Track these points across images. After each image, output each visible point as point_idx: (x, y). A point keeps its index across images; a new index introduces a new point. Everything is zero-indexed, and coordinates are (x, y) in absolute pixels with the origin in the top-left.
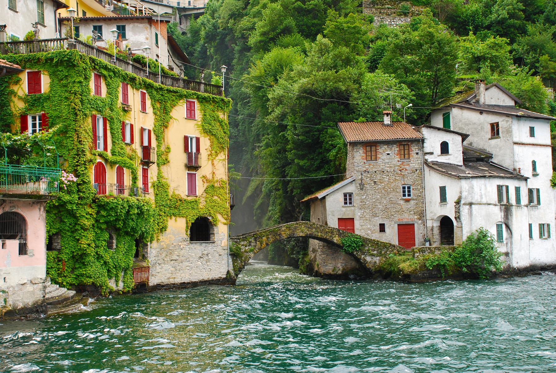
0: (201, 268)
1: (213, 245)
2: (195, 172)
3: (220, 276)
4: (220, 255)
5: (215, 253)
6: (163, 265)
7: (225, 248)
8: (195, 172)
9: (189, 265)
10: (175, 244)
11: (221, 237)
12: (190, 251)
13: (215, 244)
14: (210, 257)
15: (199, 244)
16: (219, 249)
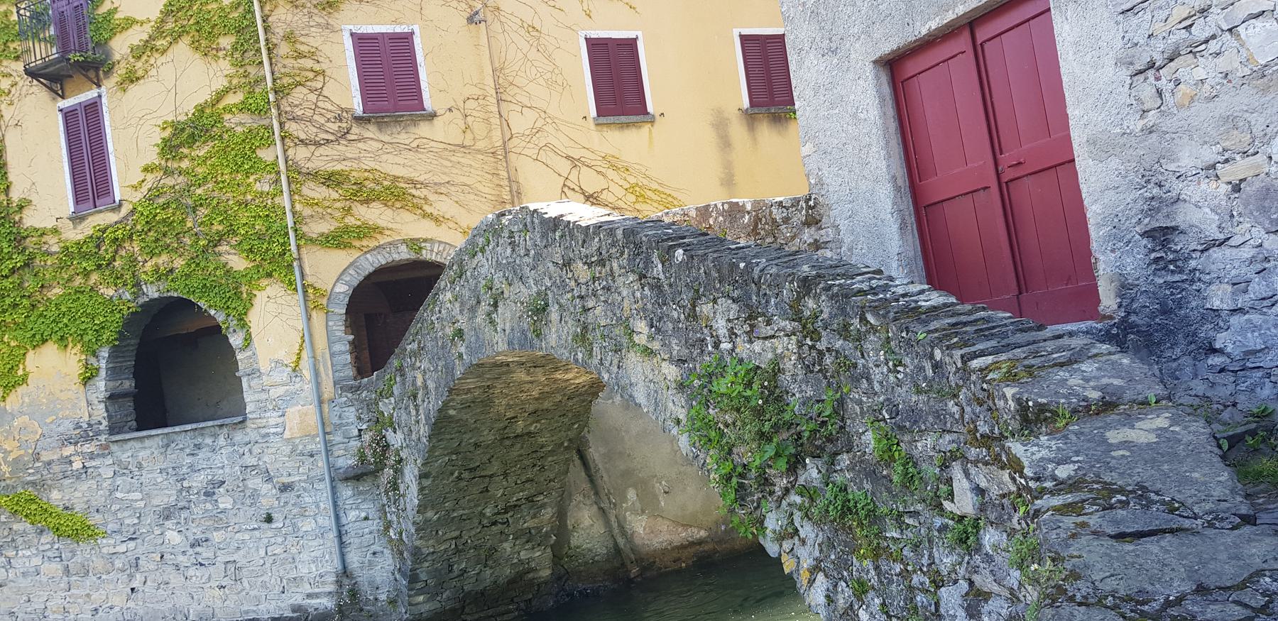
0: (181, 558)
1: (239, 436)
2: (91, 94)
3: (298, 599)
4: (285, 488)
5: (255, 482)
6: (11, 553)
7: (310, 447)
8: (91, 94)
9: (122, 548)
10: (46, 457)
11: (281, 390)
12: (119, 481)
13: (251, 433)
14: (225, 503)
15: (158, 441)
16: (276, 457)
